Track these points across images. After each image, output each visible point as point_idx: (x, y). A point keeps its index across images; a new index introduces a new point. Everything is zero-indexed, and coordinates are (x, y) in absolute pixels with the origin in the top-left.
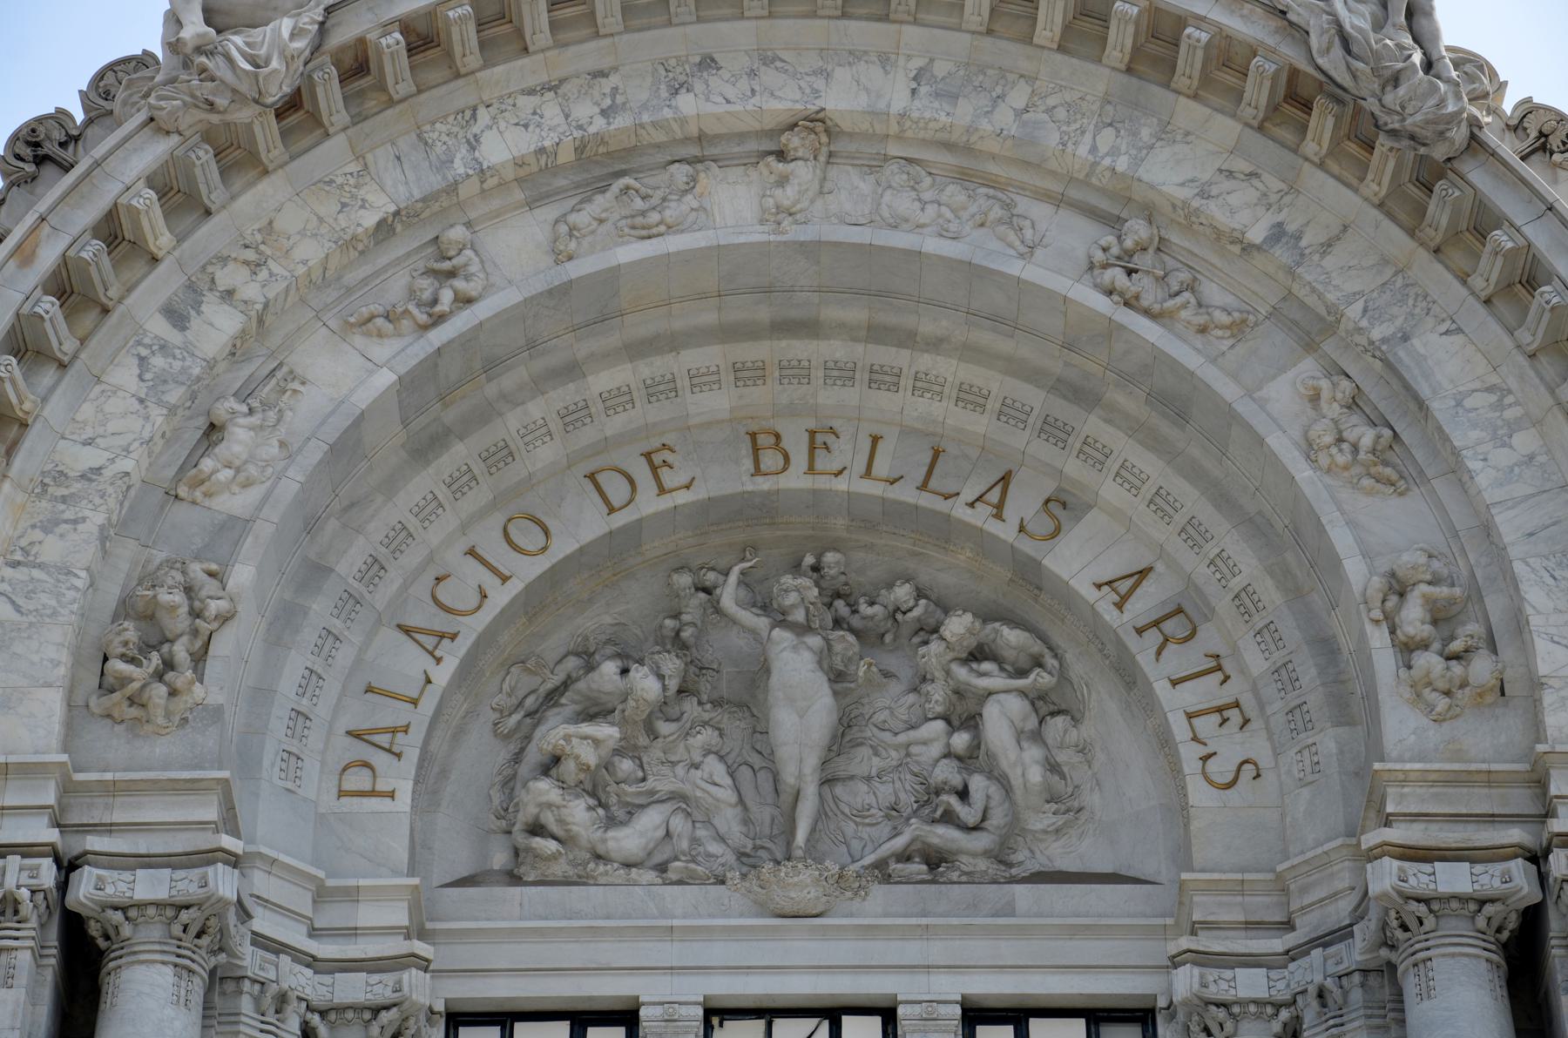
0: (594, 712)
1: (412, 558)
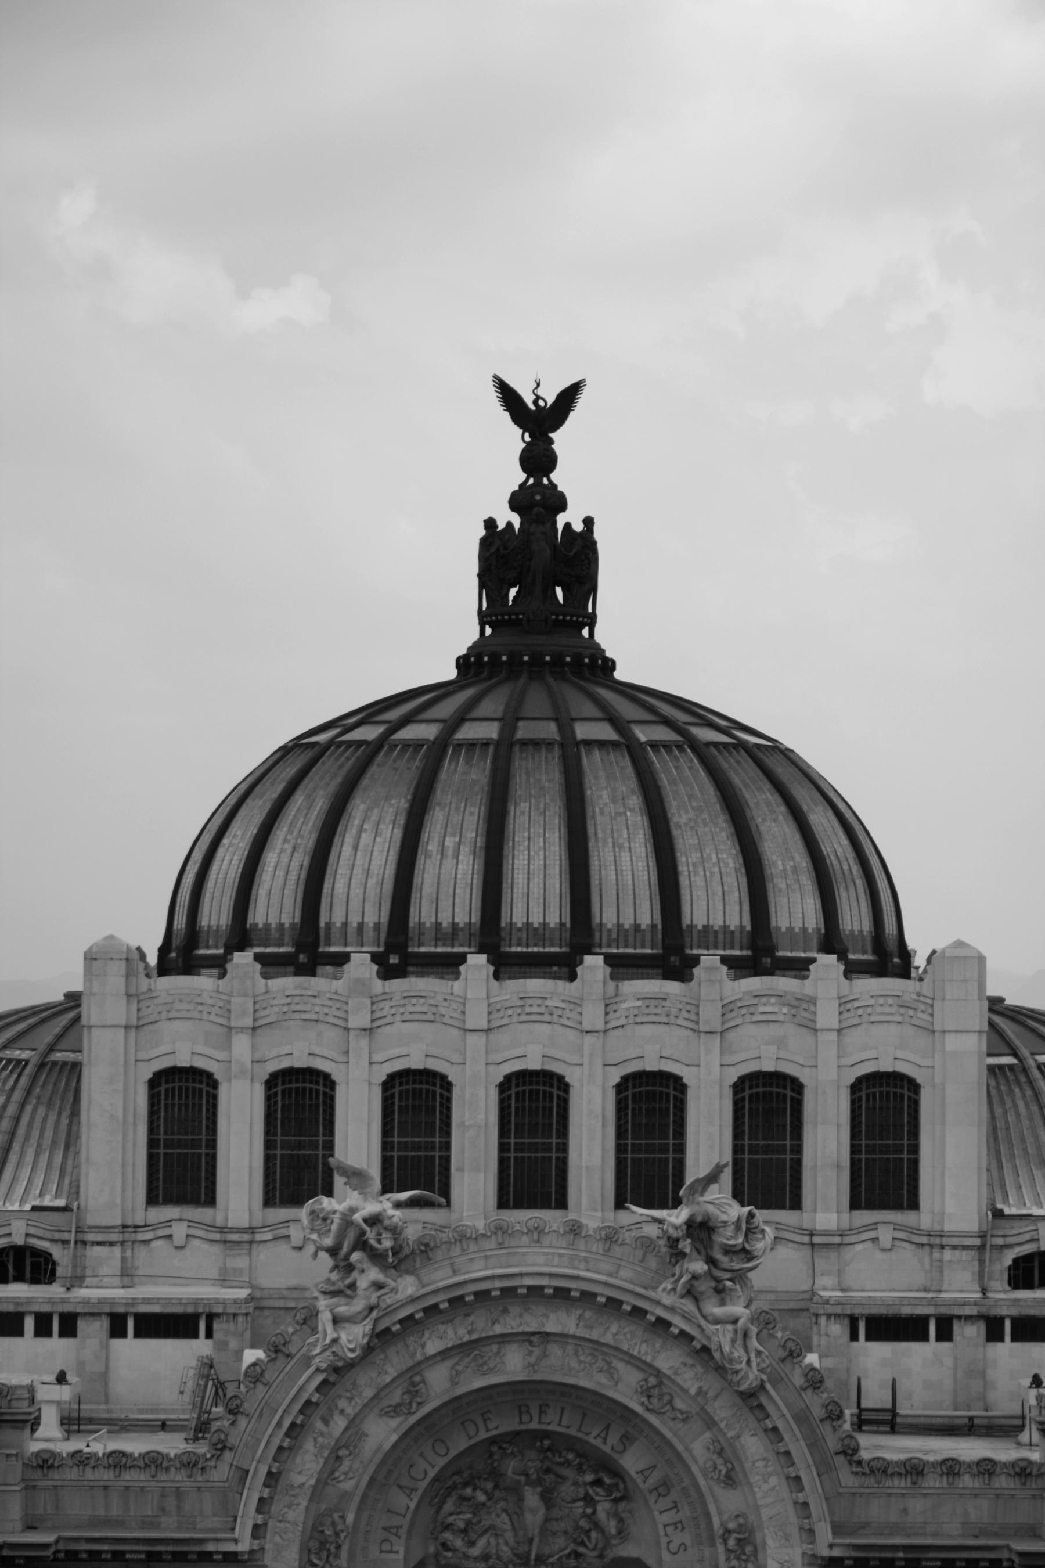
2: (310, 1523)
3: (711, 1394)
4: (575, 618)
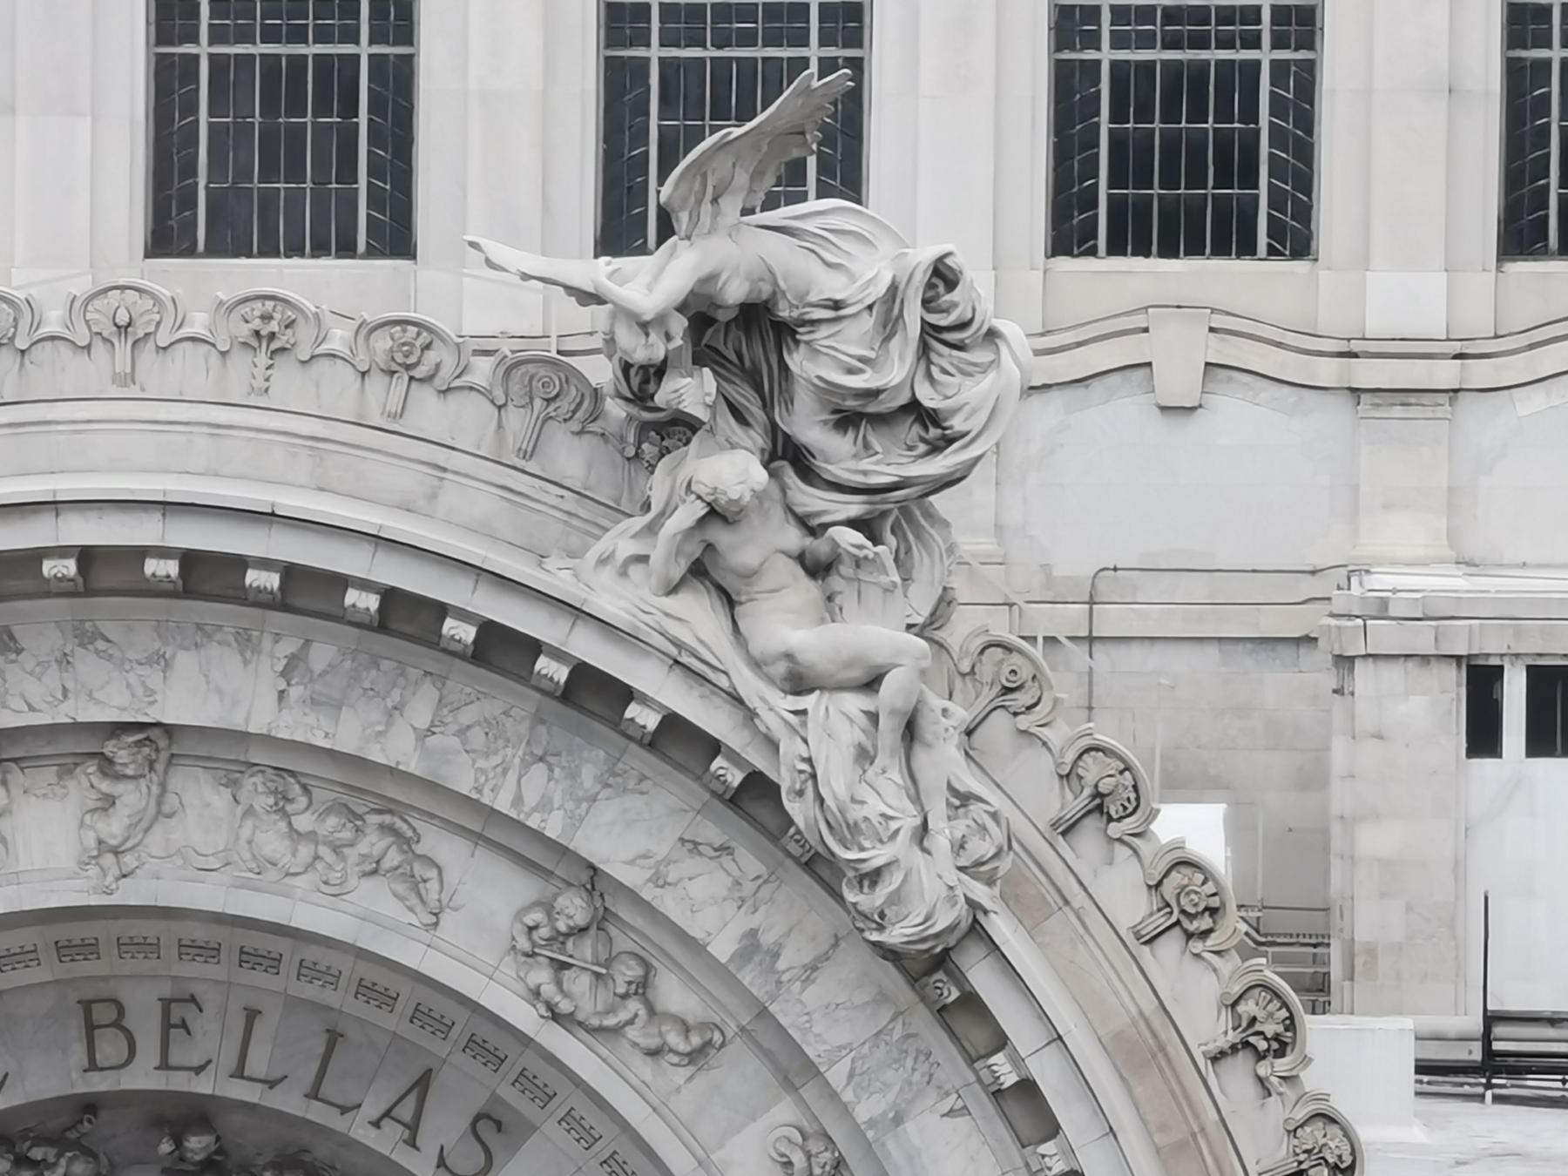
3: (792, 957)
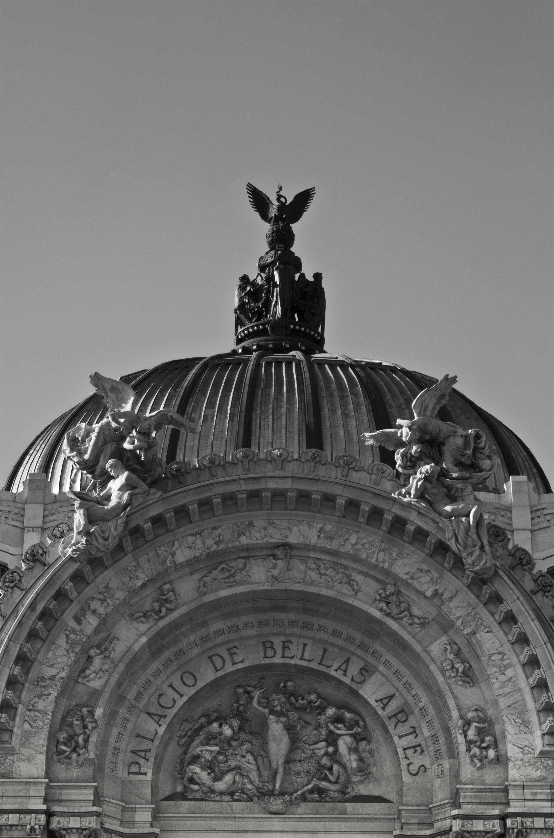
0: (211, 739)
1: (151, 690)
2: (59, 717)
4: (308, 331)
